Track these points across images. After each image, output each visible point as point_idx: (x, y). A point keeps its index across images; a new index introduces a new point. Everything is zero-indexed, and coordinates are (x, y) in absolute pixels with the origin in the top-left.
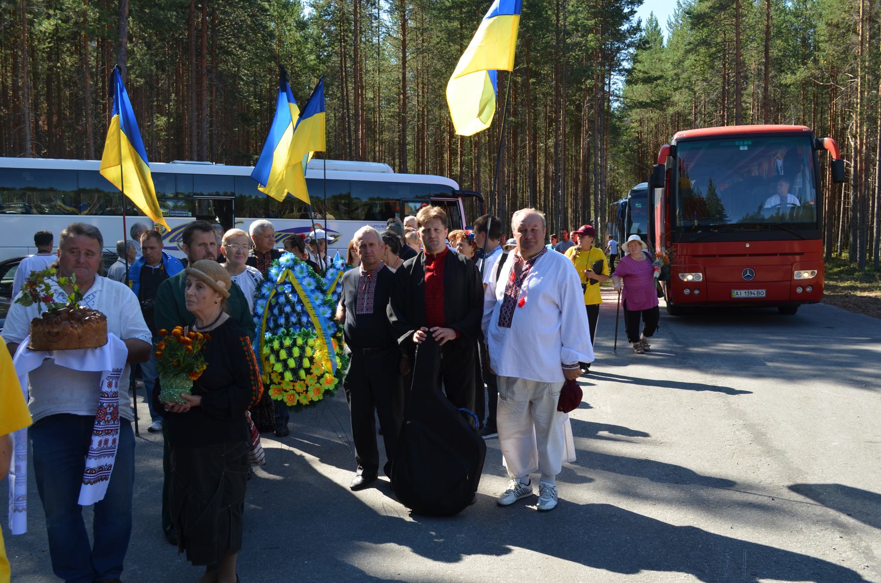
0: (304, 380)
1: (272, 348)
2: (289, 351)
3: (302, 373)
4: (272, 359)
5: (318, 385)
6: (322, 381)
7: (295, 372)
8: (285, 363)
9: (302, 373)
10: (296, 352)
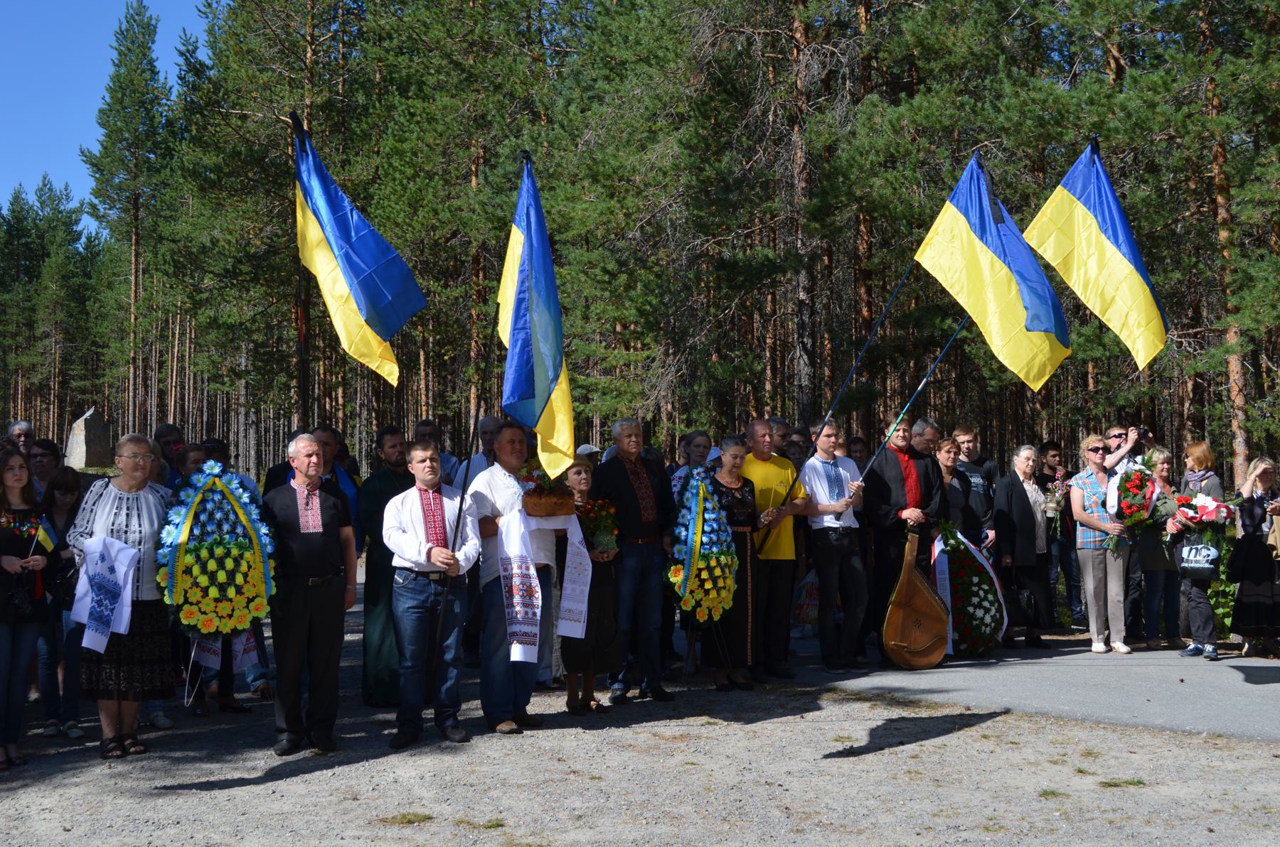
0: (231, 600)
1: (198, 558)
2: (221, 563)
3: (231, 592)
4: (196, 570)
5: (246, 611)
6: (252, 605)
7: (222, 588)
8: (212, 576)
9: (231, 592)
10: (229, 564)
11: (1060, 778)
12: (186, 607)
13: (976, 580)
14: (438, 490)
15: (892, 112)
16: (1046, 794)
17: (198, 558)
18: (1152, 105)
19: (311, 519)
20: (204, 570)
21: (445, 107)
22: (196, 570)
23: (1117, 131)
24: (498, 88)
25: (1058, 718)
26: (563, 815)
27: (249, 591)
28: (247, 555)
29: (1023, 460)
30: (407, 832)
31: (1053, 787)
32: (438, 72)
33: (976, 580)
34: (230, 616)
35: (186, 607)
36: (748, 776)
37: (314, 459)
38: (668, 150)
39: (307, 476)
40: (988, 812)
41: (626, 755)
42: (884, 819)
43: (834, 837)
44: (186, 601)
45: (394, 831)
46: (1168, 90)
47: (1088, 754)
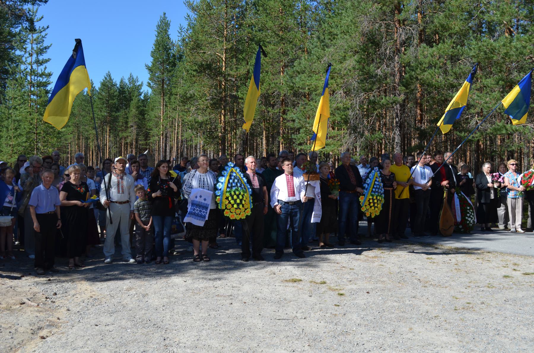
1: (231, 194)
3: (241, 206)
4: (230, 198)
7: (238, 205)
8: (235, 201)
9: (241, 206)
10: (241, 197)
11: (508, 271)
12: (226, 210)
13: (468, 208)
14: (292, 174)
15: (431, 50)
16: (506, 277)
17: (231, 194)
18: (525, 47)
19: (256, 183)
20: (233, 198)
21: (272, 49)
22: (230, 198)
23: (513, 55)
24: (291, 42)
25: (501, 253)
26: (345, 280)
27: (246, 207)
28: (245, 194)
29: (486, 167)
30: (295, 284)
31: (507, 275)
32: (271, 37)
33: (468, 208)
34: (240, 214)
35: (226, 210)
36: (402, 270)
37: (253, 164)
38: (351, 62)
39: (251, 169)
40: (488, 282)
41: (359, 262)
42: (452, 283)
43: (438, 289)
44: (226, 208)
45: (291, 284)
46: (530, 41)
47: (515, 264)
